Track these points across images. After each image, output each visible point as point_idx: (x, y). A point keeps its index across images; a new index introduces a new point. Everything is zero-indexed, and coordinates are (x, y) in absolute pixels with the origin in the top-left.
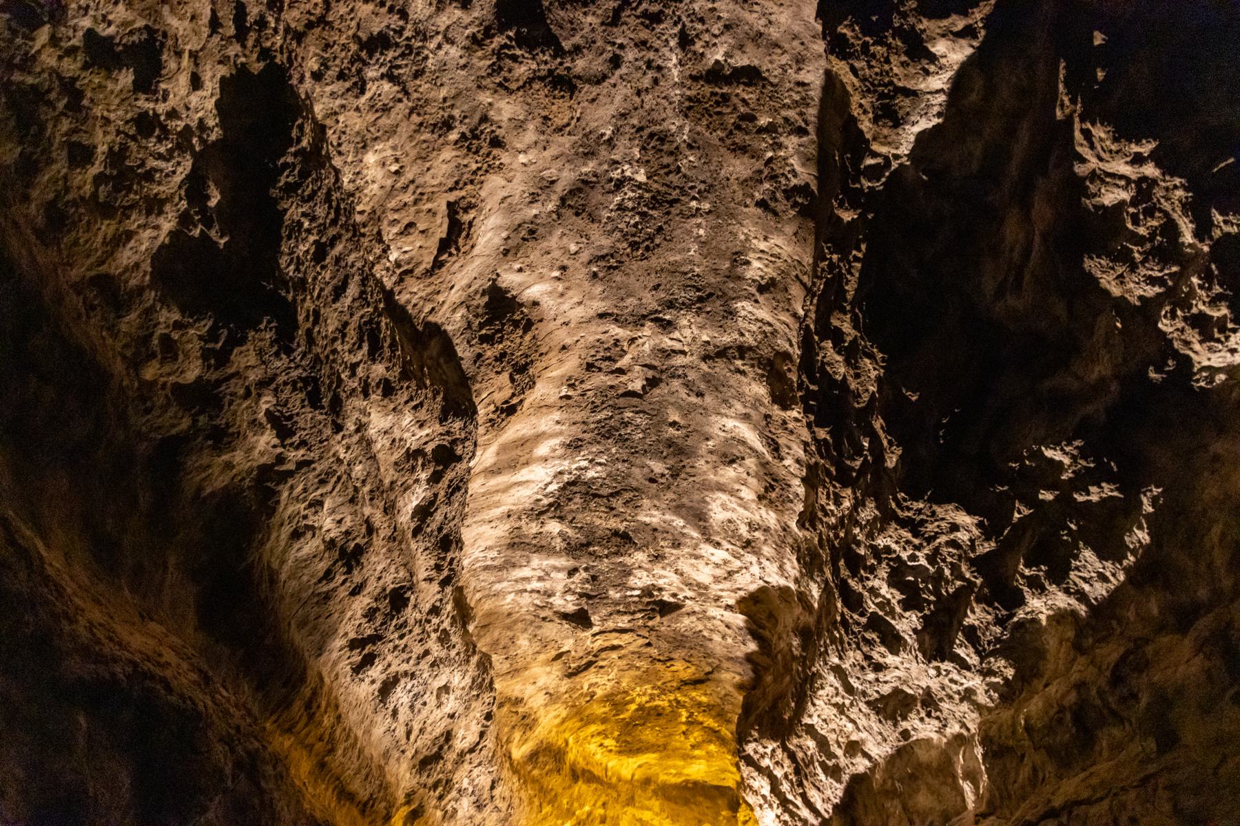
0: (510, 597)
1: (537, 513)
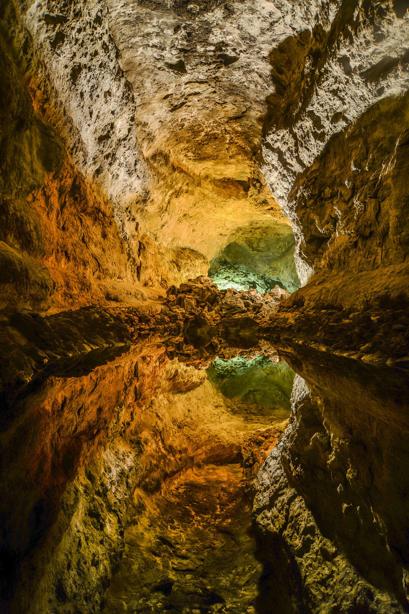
0: (141, 50)
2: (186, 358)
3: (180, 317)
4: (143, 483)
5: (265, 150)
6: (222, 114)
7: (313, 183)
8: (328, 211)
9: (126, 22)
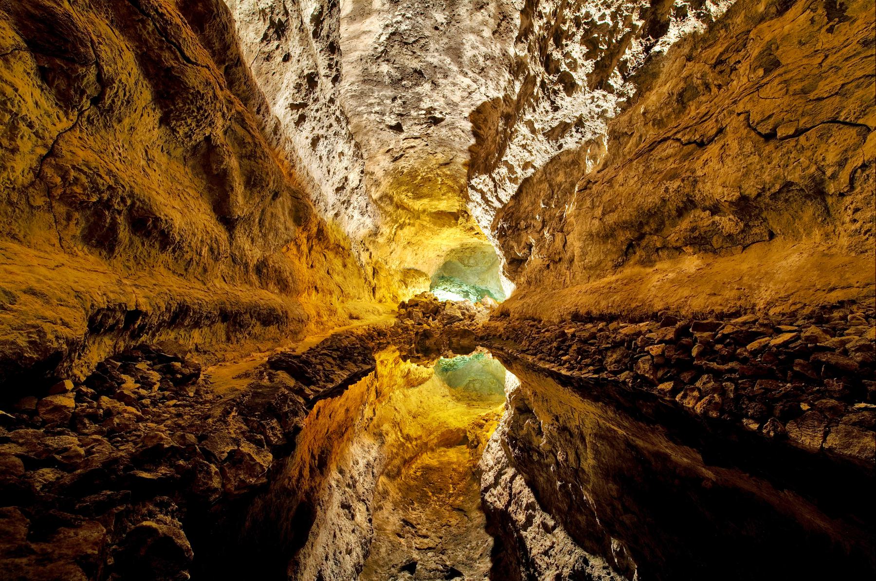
0: (365, 116)
1: (376, 59)
2: (416, 360)
3: (411, 328)
4: (386, 471)
5: (470, 191)
6: (434, 162)
7: (511, 217)
8: (524, 239)
9: (352, 96)
